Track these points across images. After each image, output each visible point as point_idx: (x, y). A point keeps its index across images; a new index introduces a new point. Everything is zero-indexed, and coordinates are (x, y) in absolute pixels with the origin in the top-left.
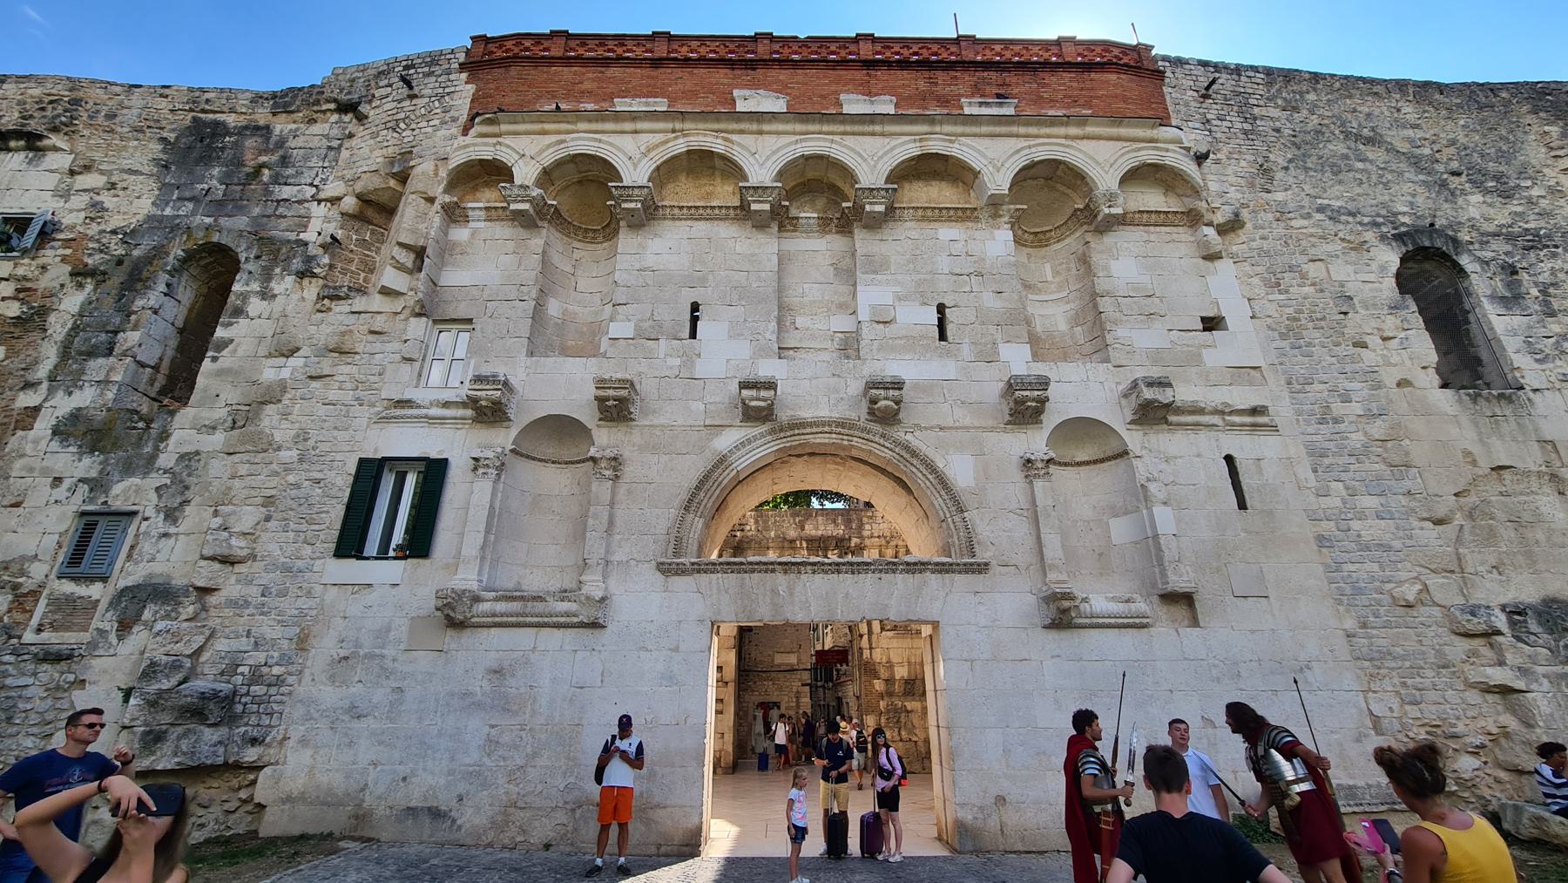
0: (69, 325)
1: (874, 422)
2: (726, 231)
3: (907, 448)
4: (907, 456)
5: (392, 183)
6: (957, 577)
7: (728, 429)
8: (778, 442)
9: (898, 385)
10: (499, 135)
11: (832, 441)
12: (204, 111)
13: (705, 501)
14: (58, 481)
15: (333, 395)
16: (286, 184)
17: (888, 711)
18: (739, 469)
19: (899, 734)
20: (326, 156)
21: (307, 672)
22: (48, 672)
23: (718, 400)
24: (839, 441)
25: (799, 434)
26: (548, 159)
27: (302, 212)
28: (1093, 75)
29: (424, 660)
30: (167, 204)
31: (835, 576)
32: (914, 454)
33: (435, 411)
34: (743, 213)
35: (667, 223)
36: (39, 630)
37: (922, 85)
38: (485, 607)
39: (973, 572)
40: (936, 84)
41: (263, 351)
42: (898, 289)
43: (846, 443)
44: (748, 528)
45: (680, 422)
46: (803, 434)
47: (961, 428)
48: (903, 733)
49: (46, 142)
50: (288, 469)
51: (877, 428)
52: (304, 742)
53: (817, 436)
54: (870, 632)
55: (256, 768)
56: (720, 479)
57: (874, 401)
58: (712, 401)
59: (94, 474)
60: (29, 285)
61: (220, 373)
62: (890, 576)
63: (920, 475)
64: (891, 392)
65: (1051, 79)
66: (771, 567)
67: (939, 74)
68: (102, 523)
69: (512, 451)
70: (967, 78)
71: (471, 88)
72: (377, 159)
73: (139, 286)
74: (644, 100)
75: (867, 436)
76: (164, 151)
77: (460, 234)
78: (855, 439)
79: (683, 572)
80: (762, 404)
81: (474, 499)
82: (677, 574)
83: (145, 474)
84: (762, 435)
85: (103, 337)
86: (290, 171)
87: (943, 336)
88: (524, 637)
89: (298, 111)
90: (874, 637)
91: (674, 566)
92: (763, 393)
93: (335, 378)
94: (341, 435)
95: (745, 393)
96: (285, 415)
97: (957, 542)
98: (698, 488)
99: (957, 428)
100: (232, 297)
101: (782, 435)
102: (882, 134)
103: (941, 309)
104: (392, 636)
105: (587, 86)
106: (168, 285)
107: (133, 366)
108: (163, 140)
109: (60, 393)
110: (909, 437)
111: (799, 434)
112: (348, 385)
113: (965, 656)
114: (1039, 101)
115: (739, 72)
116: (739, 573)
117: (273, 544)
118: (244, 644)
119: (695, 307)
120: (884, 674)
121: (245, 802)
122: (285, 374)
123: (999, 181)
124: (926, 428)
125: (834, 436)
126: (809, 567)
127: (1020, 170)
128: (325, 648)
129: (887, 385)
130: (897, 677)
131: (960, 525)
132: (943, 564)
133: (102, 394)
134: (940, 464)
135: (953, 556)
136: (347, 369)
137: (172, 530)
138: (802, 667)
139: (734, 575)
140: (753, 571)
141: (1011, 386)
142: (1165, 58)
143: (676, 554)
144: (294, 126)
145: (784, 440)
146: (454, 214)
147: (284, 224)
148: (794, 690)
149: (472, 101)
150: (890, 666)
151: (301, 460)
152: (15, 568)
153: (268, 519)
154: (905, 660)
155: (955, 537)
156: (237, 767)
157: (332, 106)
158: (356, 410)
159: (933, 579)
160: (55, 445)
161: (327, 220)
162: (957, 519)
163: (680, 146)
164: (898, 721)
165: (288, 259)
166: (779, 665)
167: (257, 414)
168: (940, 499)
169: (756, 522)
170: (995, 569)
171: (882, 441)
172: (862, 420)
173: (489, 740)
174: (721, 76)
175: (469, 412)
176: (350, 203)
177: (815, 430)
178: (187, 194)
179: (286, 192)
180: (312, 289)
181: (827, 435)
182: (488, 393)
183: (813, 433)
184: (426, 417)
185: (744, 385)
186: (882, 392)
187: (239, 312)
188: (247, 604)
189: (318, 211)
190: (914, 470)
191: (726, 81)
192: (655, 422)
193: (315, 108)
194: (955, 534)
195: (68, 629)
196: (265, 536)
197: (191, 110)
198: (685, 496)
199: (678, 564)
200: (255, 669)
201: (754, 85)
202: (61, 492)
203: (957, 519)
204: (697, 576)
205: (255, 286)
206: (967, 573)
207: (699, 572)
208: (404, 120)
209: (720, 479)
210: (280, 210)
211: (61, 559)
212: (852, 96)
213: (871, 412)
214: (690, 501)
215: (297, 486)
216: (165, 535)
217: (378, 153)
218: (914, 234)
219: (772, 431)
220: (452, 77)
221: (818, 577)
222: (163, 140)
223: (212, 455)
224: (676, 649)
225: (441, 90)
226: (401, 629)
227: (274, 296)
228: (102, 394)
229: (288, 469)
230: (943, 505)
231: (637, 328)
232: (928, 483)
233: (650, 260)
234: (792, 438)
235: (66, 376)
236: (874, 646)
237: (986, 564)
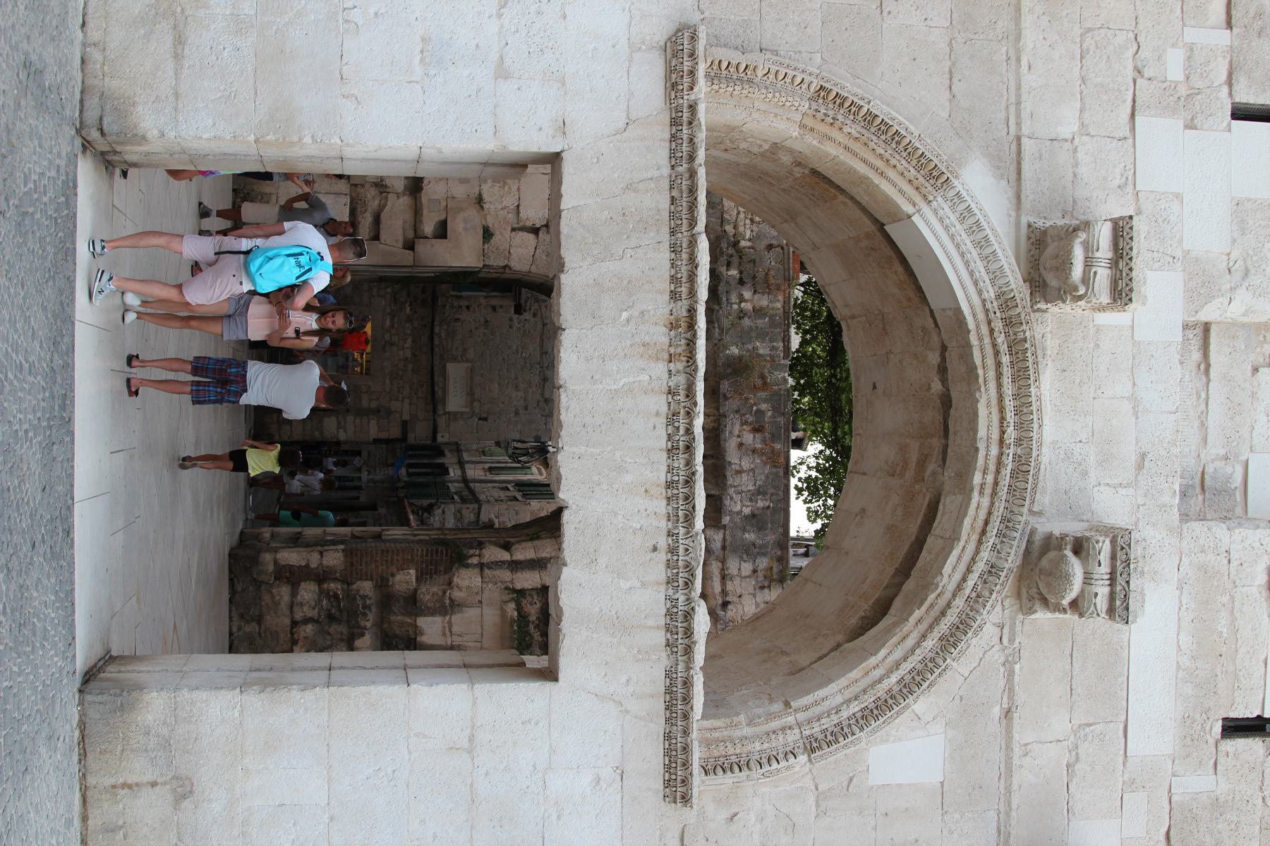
1: (1027, 552)
3: (963, 627)
4: (944, 627)
6: (658, 726)
7: (1011, 193)
8: (981, 316)
9: (1119, 608)
11: (981, 446)
13: (839, 136)
17: (350, 597)
18: (916, 219)
19: (307, 621)
23: (1083, 170)
24: (980, 462)
25: (998, 365)
31: (663, 443)
32: (949, 643)
39: (668, 768)
43: (977, 479)
44: (747, 294)
45: (1029, 80)
46: (999, 376)
47: (1009, 759)
48: (309, 629)
51: (1012, 560)
53: (995, 411)
54: (515, 566)
56: (891, 174)
57: (1079, 547)
58: (1080, 155)
63: (898, 654)
64: (1103, 590)
66: (684, 290)
75: (993, 531)
78: (986, 502)
79: (674, 85)
80: (1077, 272)
82: (670, 70)
90: (506, 575)
91: (687, 64)
92: (1103, 275)
95: (1104, 235)
97: (738, 733)
98: (870, 118)
99: (1009, 747)
101: (998, 325)
110: (990, 631)
111: (998, 365)
116: (672, 215)
120: (428, 593)
124: (1010, 674)
125: (994, 451)
126: (681, 379)
129: (1121, 581)
130: (422, 622)
131: (779, 742)
132: (687, 699)
134: (921, 705)
135: (708, 724)
138: (442, 421)
139: (665, 203)
140: (674, 249)
145: (984, 330)
148: (395, 405)
150: (447, 607)
154: (457, 640)
155: (747, 731)
162: (793, 736)
164: (331, 618)
166: (444, 374)
168: (839, 699)
169: (758, 312)
170: (676, 816)
171: (980, 566)
172: (1033, 521)
177: (1009, 404)
181: (995, 435)
183: (1001, 399)
185: (1121, 231)
186: (1105, 569)
190: (910, 642)
192: (1027, 21)
194: (757, 730)
198: (852, 89)
199: (692, 73)
203: (793, 736)
204: (666, 119)
206: (668, 752)
207: (675, 122)
209: (891, 174)
213: (1051, 544)
214: (840, 100)
219: (1006, 301)
221: (660, 403)
230: (827, 705)
232: (877, 673)
234: (989, 351)
236: (487, 571)
237: (686, 799)
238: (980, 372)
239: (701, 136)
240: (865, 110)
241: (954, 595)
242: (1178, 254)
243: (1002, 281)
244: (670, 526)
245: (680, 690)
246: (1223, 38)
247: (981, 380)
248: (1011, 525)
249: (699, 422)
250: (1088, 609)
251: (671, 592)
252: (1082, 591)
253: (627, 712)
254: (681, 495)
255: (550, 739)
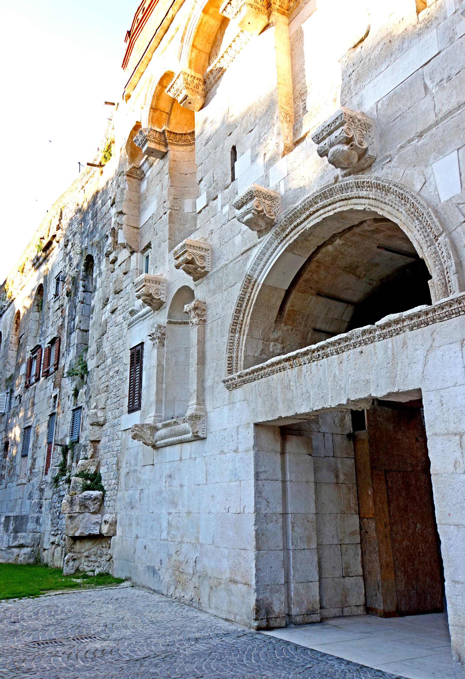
31: (325, 360)
46: (299, 225)
62: (370, 347)
69: (169, 322)
84: (270, 243)
93: (118, 309)
106: (84, 286)
107: (81, 333)
113: (452, 427)
140: (273, 372)
143: (230, 372)
207: (244, 382)
214: (235, 324)
215: (112, 377)
224: (236, 451)
238: (300, 233)
239: (247, 370)
240: (235, 314)
241: (369, 198)
242: (265, 174)
243: (272, 240)
244: (351, 348)
245: (415, 320)
246: (219, 196)
247: (302, 231)
248: (341, 189)
249: (313, 347)
250: (342, 136)
251: (377, 339)
252: (338, 143)
253: (431, 346)
254: (339, 346)
255: (449, 387)
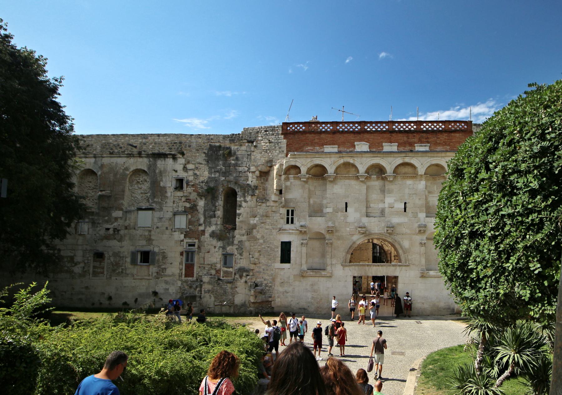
0: (203, 210)
2: (353, 182)
3: (394, 240)
5: (268, 168)
10: (296, 158)
12: (211, 142)
14: (215, 247)
15: (267, 227)
16: (240, 166)
20: (248, 158)
21: (276, 285)
22: (229, 285)
26: (309, 165)
27: (246, 175)
28: (452, 134)
29: (297, 283)
30: (212, 173)
32: (396, 241)
33: (291, 231)
34: (357, 178)
35: (339, 180)
36: (223, 277)
37: (405, 139)
38: (309, 273)
40: (409, 138)
41: (249, 216)
42: (395, 198)
49: (177, 156)
50: (262, 244)
52: (278, 297)
55: (271, 302)
59: (222, 245)
60: (188, 198)
61: (241, 222)
65: (440, 136)
67: (410, 135)
68: (228, 257)
70: (418, 136)
71: (285, 140)
72: (263, 160)
73: (215, 199)
74: (332, 146)
76: (206, 156)
77: (288, 183)
81: (303, 251)
83: (233, 246)
85: (212, 213)
86: (240, 162)
87: (405, 211)
88: (316, 279)
89: (237, 142)
92: (363, 229)
94: (271, 236)
96: (258, 232)
100: (238, 203)
102: (394, 157)
103: (405, 203)
104: (291, 278)
105: (316, 141)
108: (204, 153)
109: (208, 227)
112: (270, 224)
114: (436, 144)
115: (356, 135)
117: (263, 260)
118: (262, 280)
119: (346, 203)
121: (269, 307)
122: (255, 222)
123: (421, 171)
127: (429, 167)
128: (278, 281)
133: (217, 227)
134: (402, 243)
136: (268, 220)
137: (242, 257)
141: (420, 226)
142: (475, 125)
144: (236, 147)
146: (287, 179)
147: (242, 179)
149: (287, 146)
151: (264, 242)
152: (214, 265)
153: (260, 255)
156: (268, 301)
157: (246, 141)
158: (273, 231)
159: (398, 268)
160: (211, 239)
161: (253, 178)
163: (342, 161)
165: (248, 191)
167: (252, 232)
170: (411, 266)
173: (312, 297)
174: (351, 137)
175: (298, 232)
176: (257, 173)
178: (216, 170)
179: (240, 169)
180: (255, 199)
182: (303, 230)
184: (289, 232)
187: (240, 206)
188: (261, 272)
189: (250, 175)
191: (352, 138)
193: (241, 141)
195: (228, 277)
196: (261, 259)
197: (208, 142)
200: (266, 284)
201: (360, 140)
202: (217, 249)
205: (242, 199)
208: (269, 149)
210: (240, 175)
211: (222, 263)
212: (386, 144)
214: (348, 251)
216: (241, 258)
217: (262, 159)
218: (400, 182)
219: (365, 236)
220: (280, 136)
222: (204, 153)
223: (245, 241)
225: (277, 141)
226: (292, 277)
227: (247, 202)
228: (217, 227)
229: (262, 244)
231: (333, 209)
233: (335, 191)
235: (208, 223)
246: (339, 213)
